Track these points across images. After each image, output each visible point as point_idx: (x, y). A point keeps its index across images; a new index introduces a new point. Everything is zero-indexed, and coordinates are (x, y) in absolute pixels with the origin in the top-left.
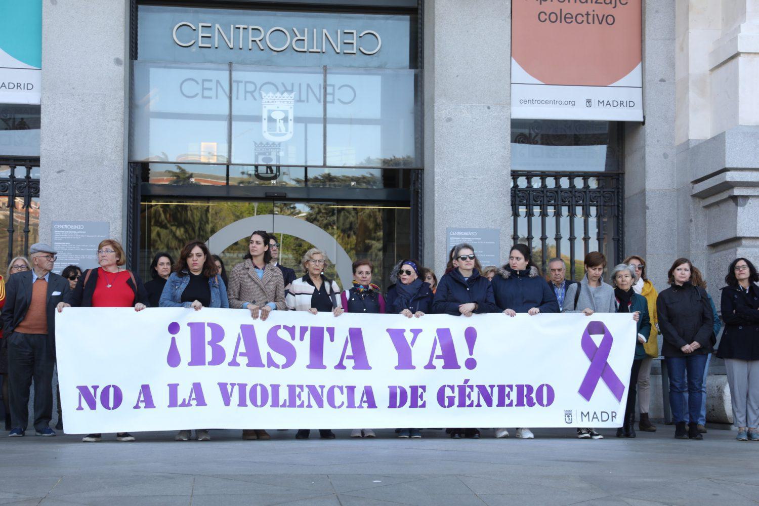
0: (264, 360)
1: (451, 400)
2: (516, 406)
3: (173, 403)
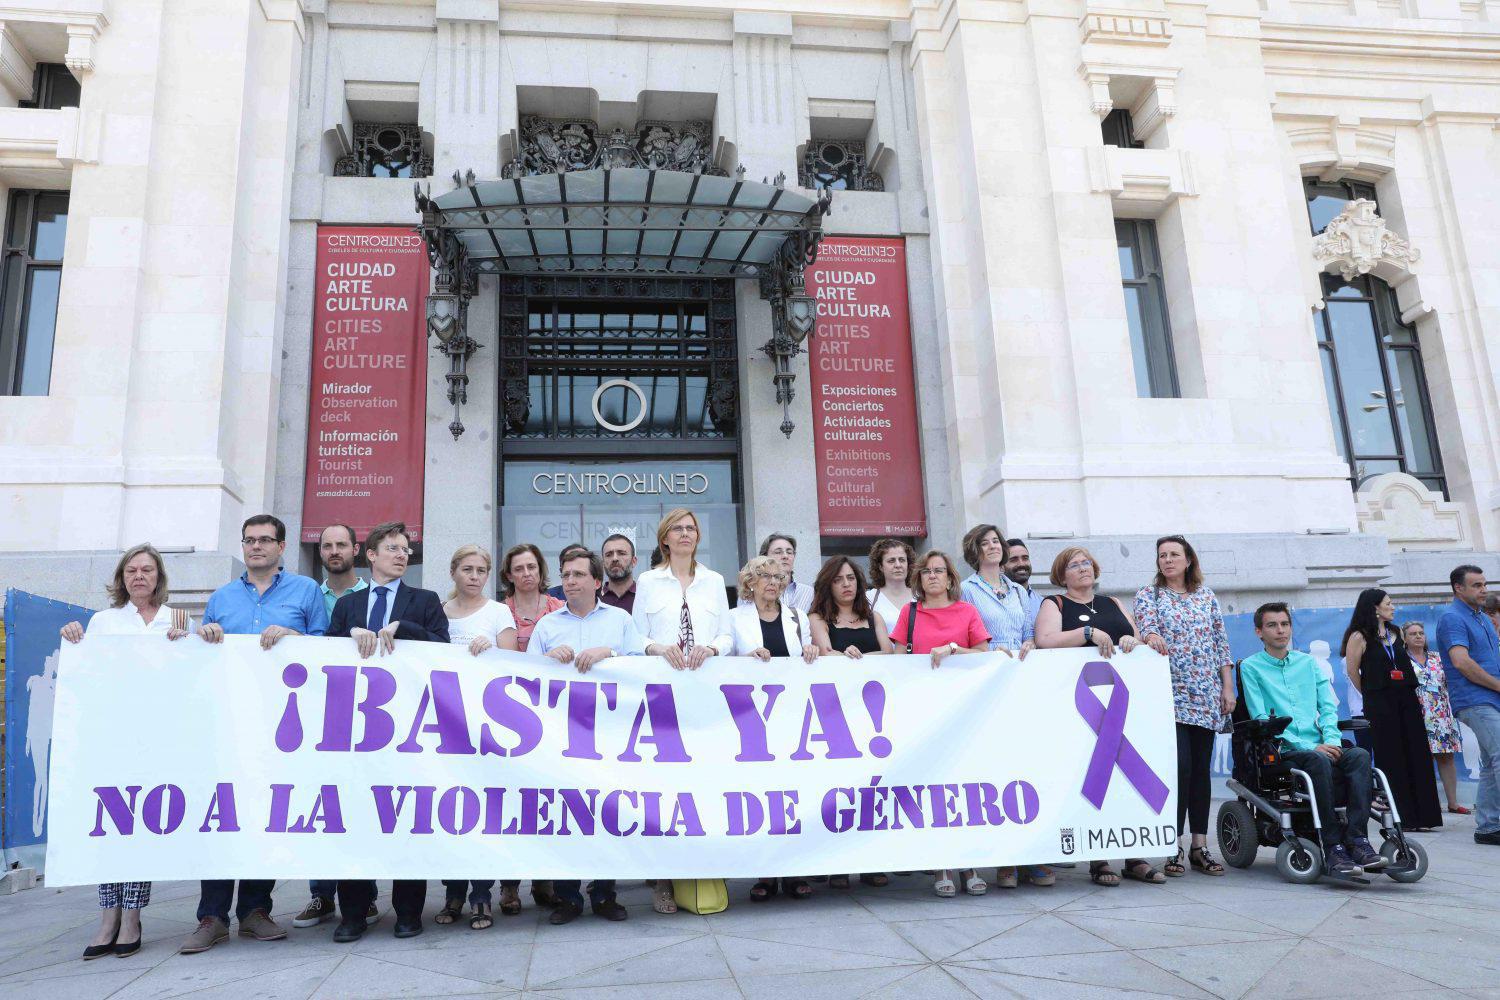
0: (476, 742)
1: (848, 815)
2: (968, 824)
3: (277, 822)
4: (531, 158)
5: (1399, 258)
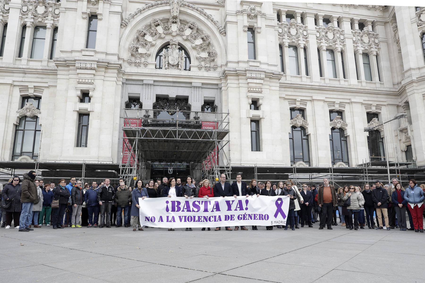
5: (305, 124)
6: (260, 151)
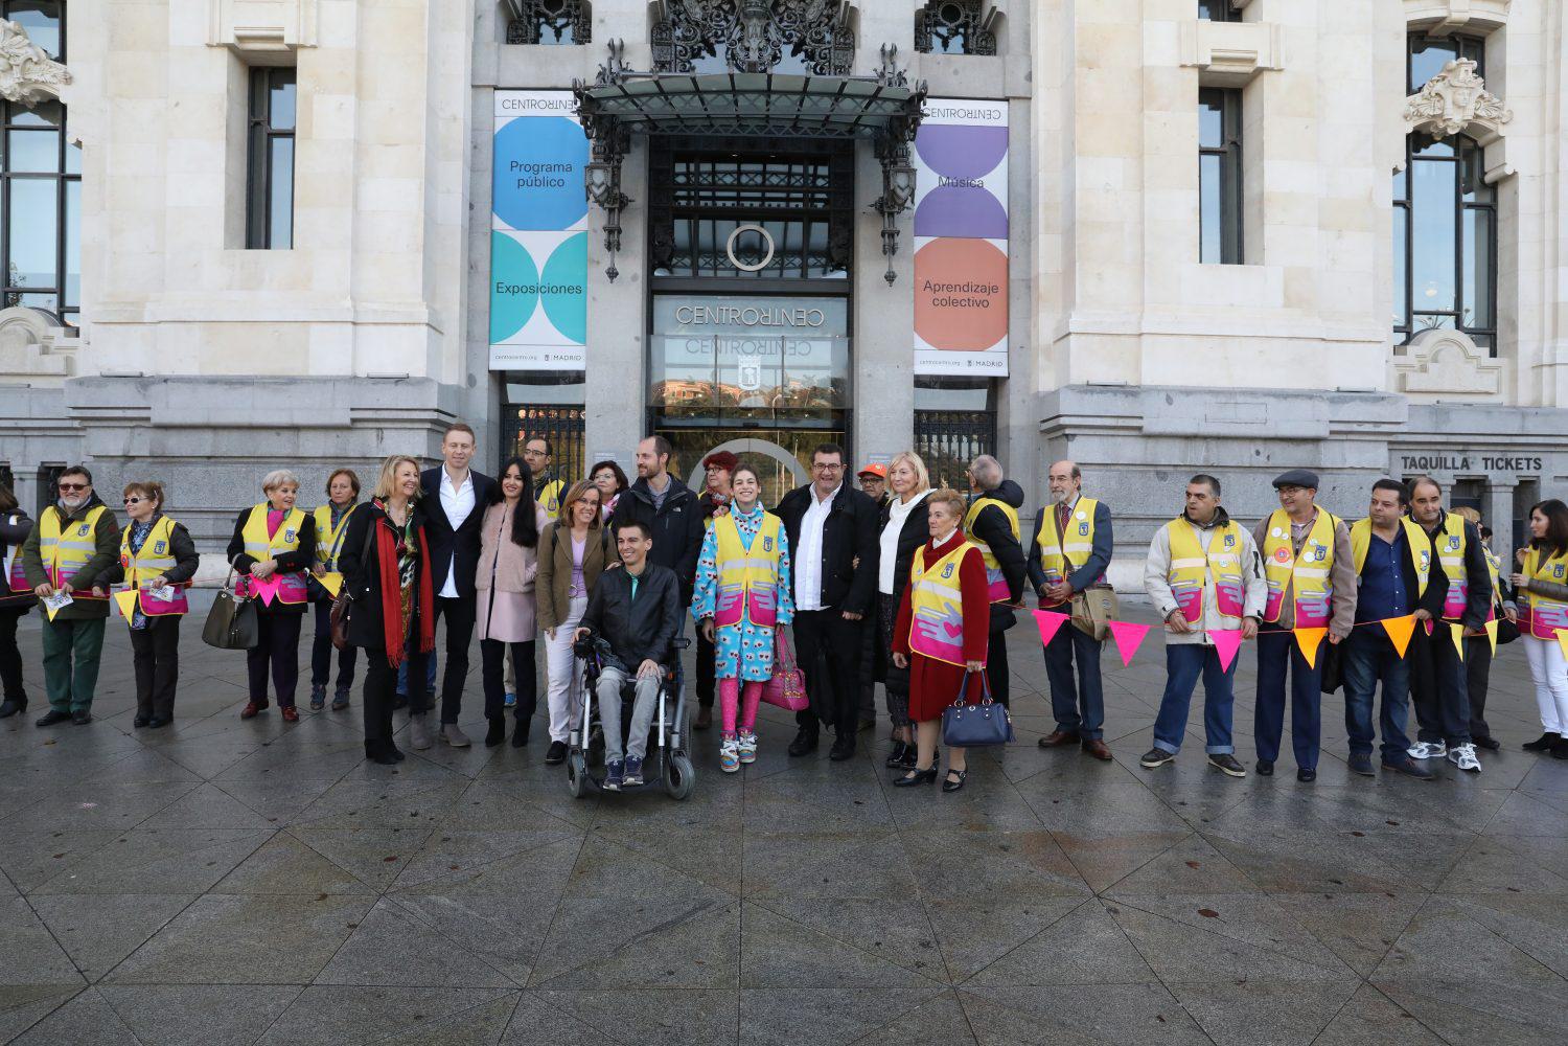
4: (677, 20)
6: (1240, 261)
